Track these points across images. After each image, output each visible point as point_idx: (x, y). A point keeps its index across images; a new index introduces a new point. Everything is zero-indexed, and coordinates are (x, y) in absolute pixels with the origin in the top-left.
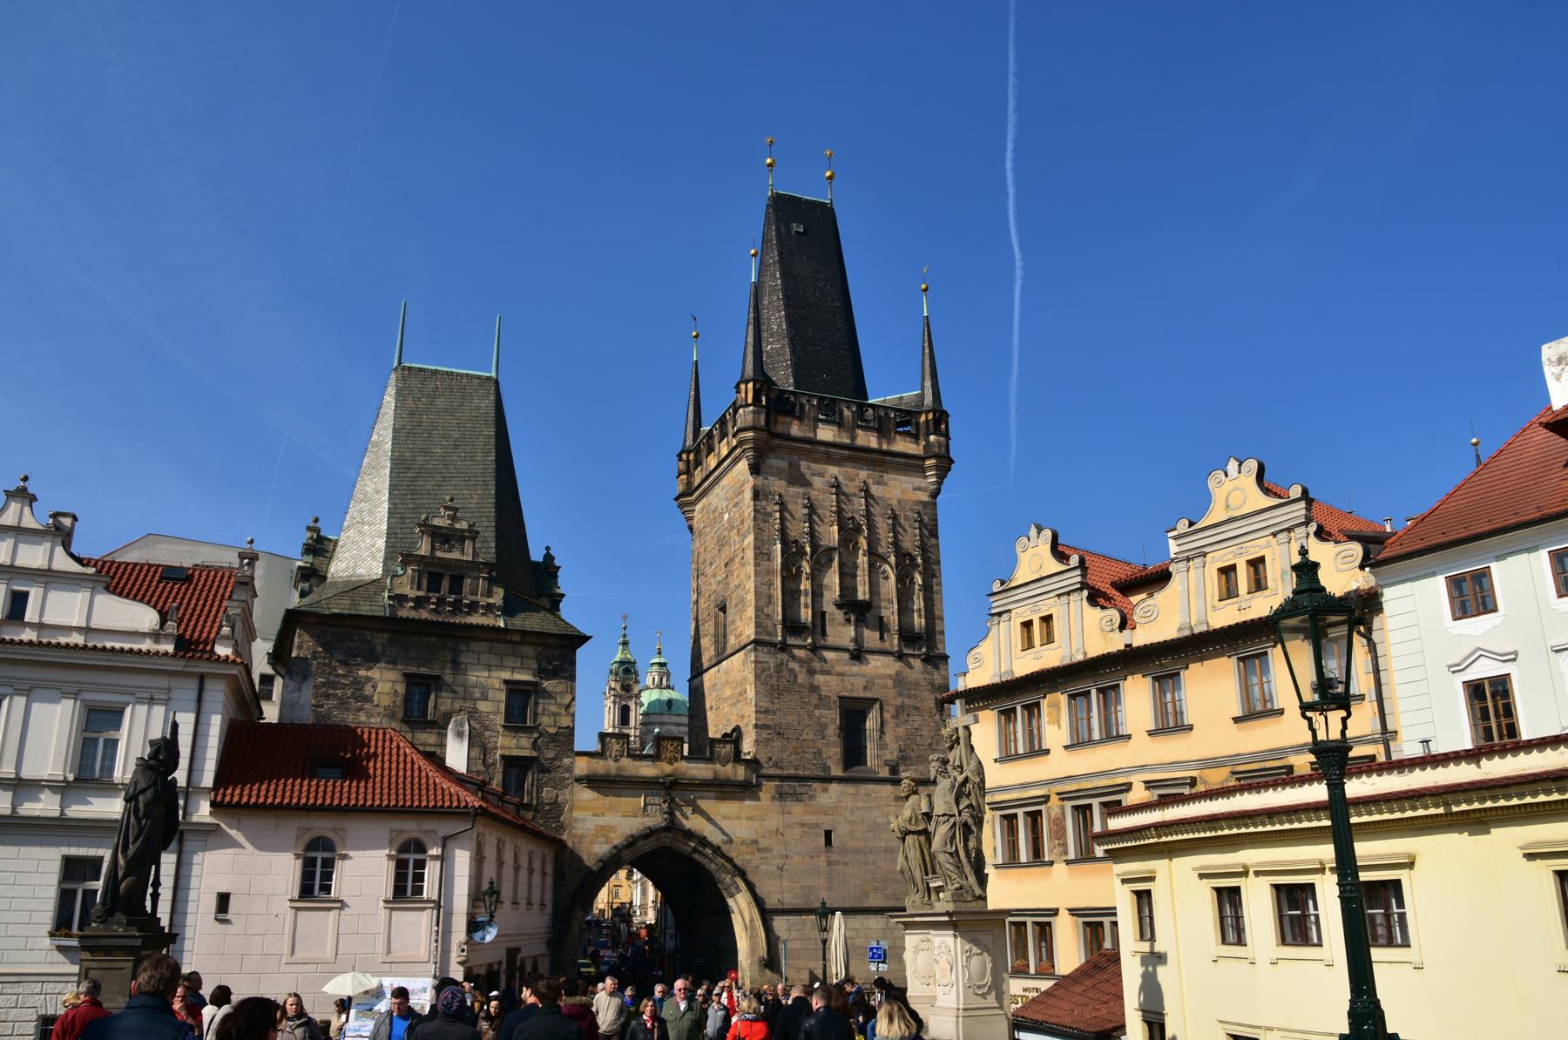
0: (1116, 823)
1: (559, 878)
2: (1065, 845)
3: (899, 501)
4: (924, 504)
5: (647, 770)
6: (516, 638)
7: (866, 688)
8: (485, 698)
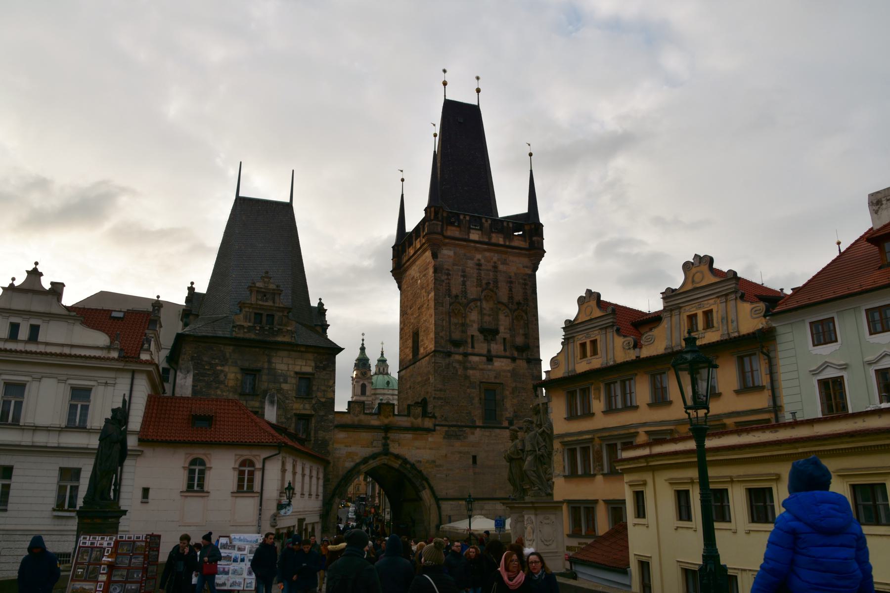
0: (626, 454)
1: (326, 480)
2: (602, 465)
3: (515, 274)
5: (375, 422)
6: (303, 349)
7: (496, 377)
8: (286, 382)
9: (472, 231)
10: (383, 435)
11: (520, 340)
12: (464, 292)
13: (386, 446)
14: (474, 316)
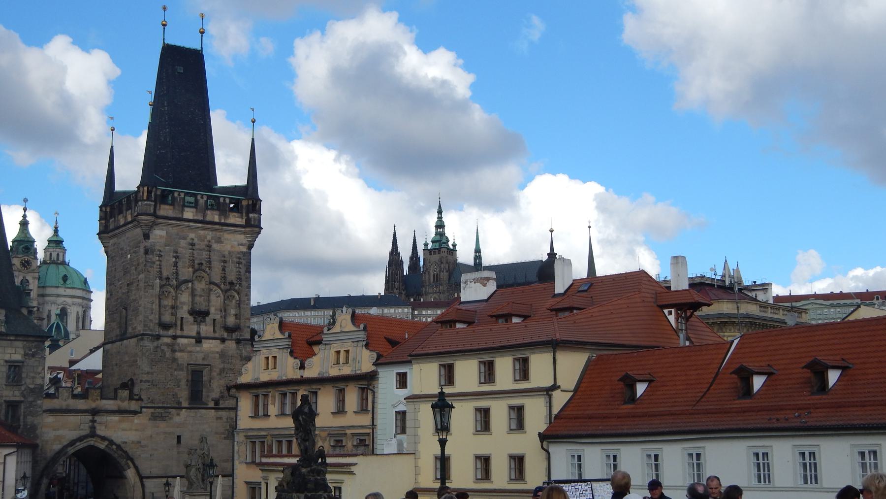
0: (264, 460)
1: (35, 463)
3: (229, 253)
4: (244, 253)
7: (203, 359)
9: (186, 209)
10: (90, 418)
11: (231, 321)
12: (177, 274)
13: (93, 428)
14: (185, 297)
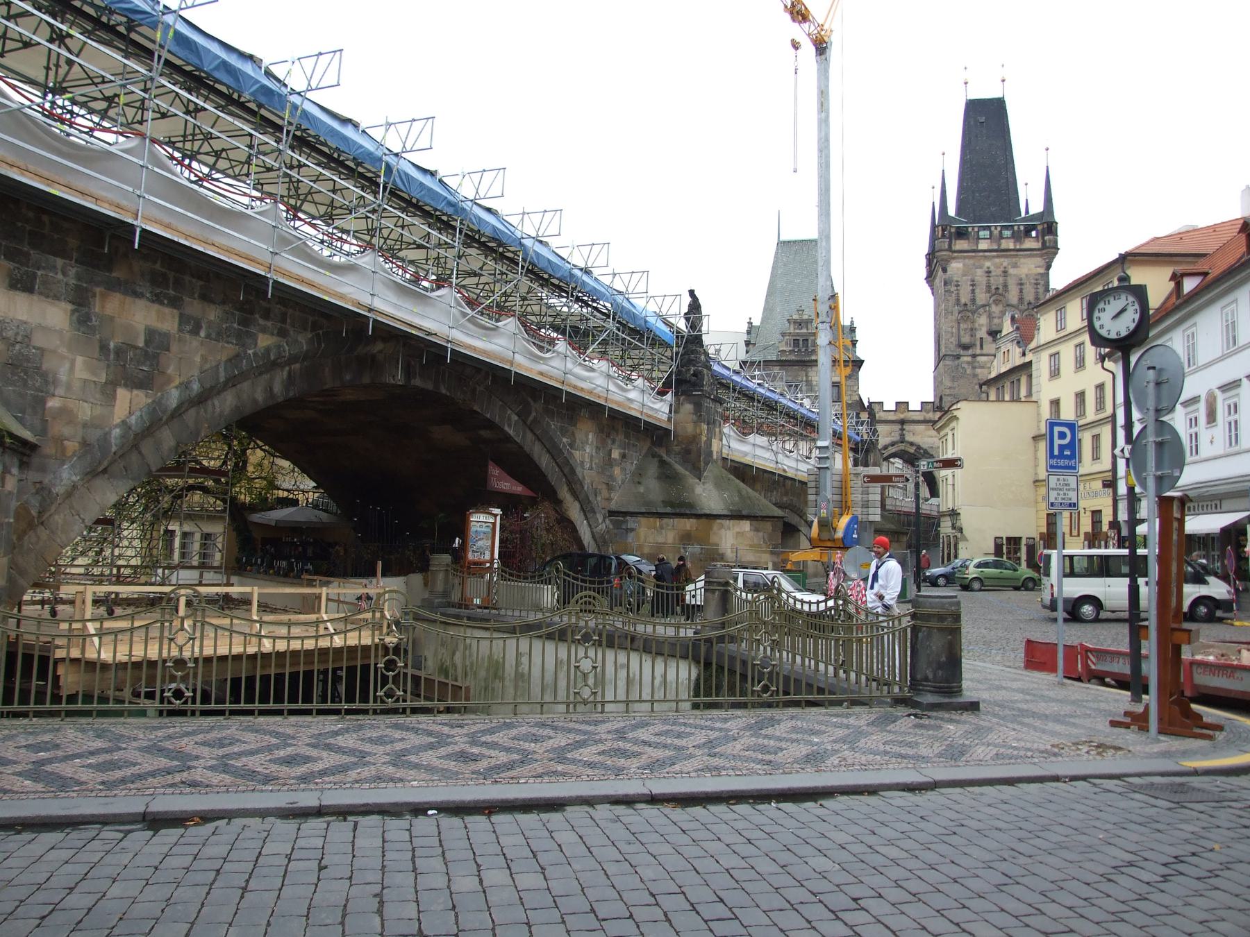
5: (892, 417)
12: (973, 300)
13: (902, 435)
14: (983, 320)
